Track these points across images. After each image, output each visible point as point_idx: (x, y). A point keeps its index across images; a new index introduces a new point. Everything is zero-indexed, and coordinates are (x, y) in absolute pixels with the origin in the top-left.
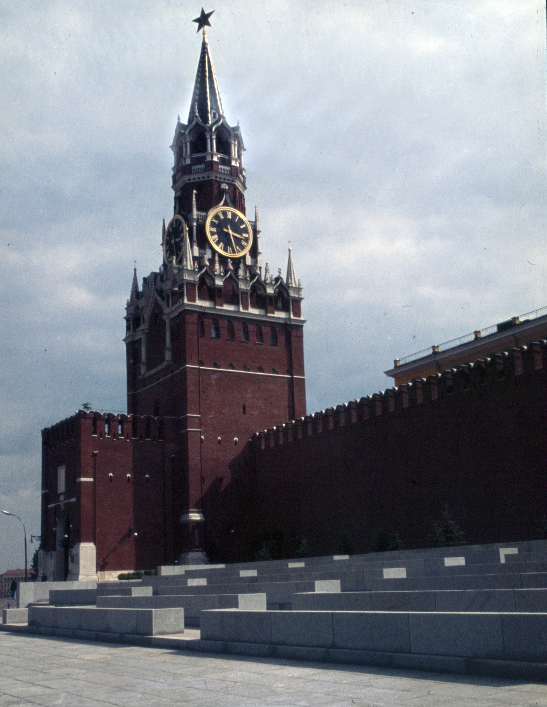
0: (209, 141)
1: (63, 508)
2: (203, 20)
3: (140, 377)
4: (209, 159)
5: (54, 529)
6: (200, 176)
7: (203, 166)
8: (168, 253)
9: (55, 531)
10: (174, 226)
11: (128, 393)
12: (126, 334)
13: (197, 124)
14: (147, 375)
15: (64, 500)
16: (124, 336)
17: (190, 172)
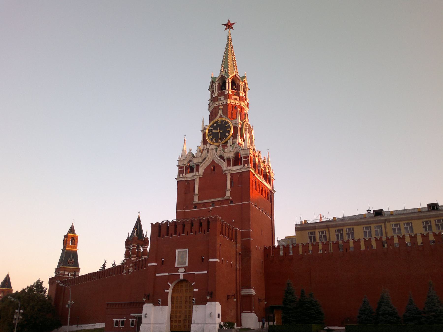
0: (241, 86)
1: (181, 277)
2: (229, 26)
3: (194, 202)
4: (241, 95)
5: (166, 291)
6: (237, 102)
7: (238, 97)
8: (211, 136)
9: (168, 292)
10: (220, 123)
11: (177, 210)
12: (179, 175)
13: (235, 75)
14: (200, 202)
15: (185, 272)
16: (176, 176)
17: (231, 99)
